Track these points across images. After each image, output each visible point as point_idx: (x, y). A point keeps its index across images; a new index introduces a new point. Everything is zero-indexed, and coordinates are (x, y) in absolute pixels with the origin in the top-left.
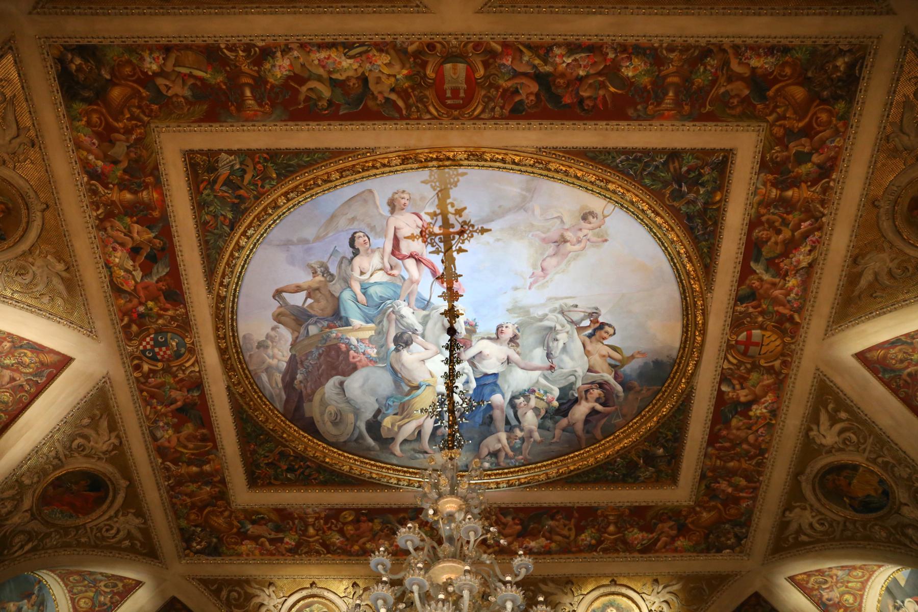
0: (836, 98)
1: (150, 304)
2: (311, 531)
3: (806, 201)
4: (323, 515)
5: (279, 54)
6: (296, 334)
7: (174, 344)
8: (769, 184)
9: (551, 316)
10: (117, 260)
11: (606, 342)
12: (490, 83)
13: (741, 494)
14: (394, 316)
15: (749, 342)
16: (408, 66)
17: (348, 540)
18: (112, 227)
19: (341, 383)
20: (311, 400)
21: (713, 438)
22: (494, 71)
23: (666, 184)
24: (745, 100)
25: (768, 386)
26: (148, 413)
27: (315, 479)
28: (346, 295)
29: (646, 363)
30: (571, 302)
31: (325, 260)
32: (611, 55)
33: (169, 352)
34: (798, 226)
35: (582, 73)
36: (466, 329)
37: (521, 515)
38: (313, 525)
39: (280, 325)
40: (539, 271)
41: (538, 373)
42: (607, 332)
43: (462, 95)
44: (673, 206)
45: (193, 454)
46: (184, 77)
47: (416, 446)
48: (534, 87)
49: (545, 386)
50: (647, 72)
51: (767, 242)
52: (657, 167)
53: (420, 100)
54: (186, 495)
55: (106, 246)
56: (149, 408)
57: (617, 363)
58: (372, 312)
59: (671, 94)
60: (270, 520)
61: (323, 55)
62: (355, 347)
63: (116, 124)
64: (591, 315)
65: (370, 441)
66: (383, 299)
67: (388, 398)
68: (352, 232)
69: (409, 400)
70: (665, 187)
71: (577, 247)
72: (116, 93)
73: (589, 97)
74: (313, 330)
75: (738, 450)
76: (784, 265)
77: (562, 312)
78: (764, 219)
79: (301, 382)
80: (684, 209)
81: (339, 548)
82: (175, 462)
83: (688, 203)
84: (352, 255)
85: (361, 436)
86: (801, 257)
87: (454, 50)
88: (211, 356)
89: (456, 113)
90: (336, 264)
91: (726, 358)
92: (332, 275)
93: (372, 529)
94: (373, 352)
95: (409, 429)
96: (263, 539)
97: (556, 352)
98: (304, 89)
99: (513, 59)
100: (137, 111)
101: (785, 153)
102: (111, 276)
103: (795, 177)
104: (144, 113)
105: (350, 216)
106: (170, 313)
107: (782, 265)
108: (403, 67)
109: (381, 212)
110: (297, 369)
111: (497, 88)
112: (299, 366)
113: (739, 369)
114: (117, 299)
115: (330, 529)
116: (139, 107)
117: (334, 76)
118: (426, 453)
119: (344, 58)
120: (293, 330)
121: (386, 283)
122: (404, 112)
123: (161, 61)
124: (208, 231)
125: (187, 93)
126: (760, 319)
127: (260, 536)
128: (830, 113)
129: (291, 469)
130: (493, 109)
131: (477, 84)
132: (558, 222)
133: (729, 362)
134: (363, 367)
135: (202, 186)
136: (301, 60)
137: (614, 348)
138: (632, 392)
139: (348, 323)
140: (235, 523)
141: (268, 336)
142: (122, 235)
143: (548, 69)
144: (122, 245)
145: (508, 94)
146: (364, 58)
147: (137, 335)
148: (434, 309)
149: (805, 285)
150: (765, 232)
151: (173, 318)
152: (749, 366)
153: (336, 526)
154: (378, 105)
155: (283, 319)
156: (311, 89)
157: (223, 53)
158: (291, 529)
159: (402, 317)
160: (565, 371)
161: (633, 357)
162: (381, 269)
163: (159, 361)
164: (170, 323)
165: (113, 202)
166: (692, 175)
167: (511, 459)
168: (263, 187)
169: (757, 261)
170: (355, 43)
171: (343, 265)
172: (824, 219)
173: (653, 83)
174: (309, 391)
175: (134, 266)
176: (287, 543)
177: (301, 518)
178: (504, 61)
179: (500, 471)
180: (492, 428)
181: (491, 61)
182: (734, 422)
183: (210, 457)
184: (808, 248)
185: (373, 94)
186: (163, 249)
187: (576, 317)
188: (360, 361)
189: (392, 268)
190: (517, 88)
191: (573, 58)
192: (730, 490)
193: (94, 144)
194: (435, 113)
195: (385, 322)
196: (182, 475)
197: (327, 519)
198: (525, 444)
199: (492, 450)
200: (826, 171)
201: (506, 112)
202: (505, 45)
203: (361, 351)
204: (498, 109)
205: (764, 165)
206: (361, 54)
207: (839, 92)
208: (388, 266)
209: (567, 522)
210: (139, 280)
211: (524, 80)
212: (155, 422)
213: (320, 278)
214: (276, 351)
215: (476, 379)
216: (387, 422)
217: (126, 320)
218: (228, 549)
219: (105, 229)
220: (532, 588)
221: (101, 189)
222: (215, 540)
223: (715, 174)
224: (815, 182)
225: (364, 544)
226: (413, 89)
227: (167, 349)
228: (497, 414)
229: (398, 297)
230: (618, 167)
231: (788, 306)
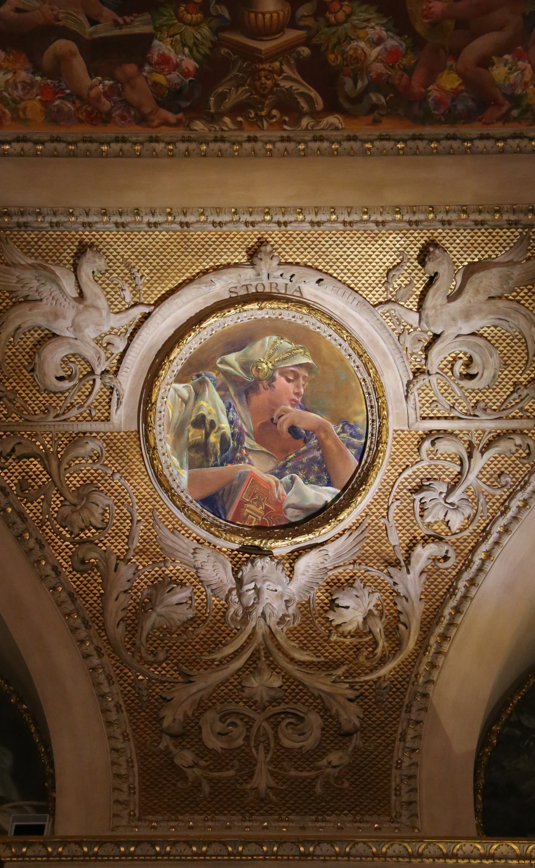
17: (417, 44)
81: (378, 84)
96: (62, 45)
127: (53, 31)
176: (165, 60)
225: (485, 62)
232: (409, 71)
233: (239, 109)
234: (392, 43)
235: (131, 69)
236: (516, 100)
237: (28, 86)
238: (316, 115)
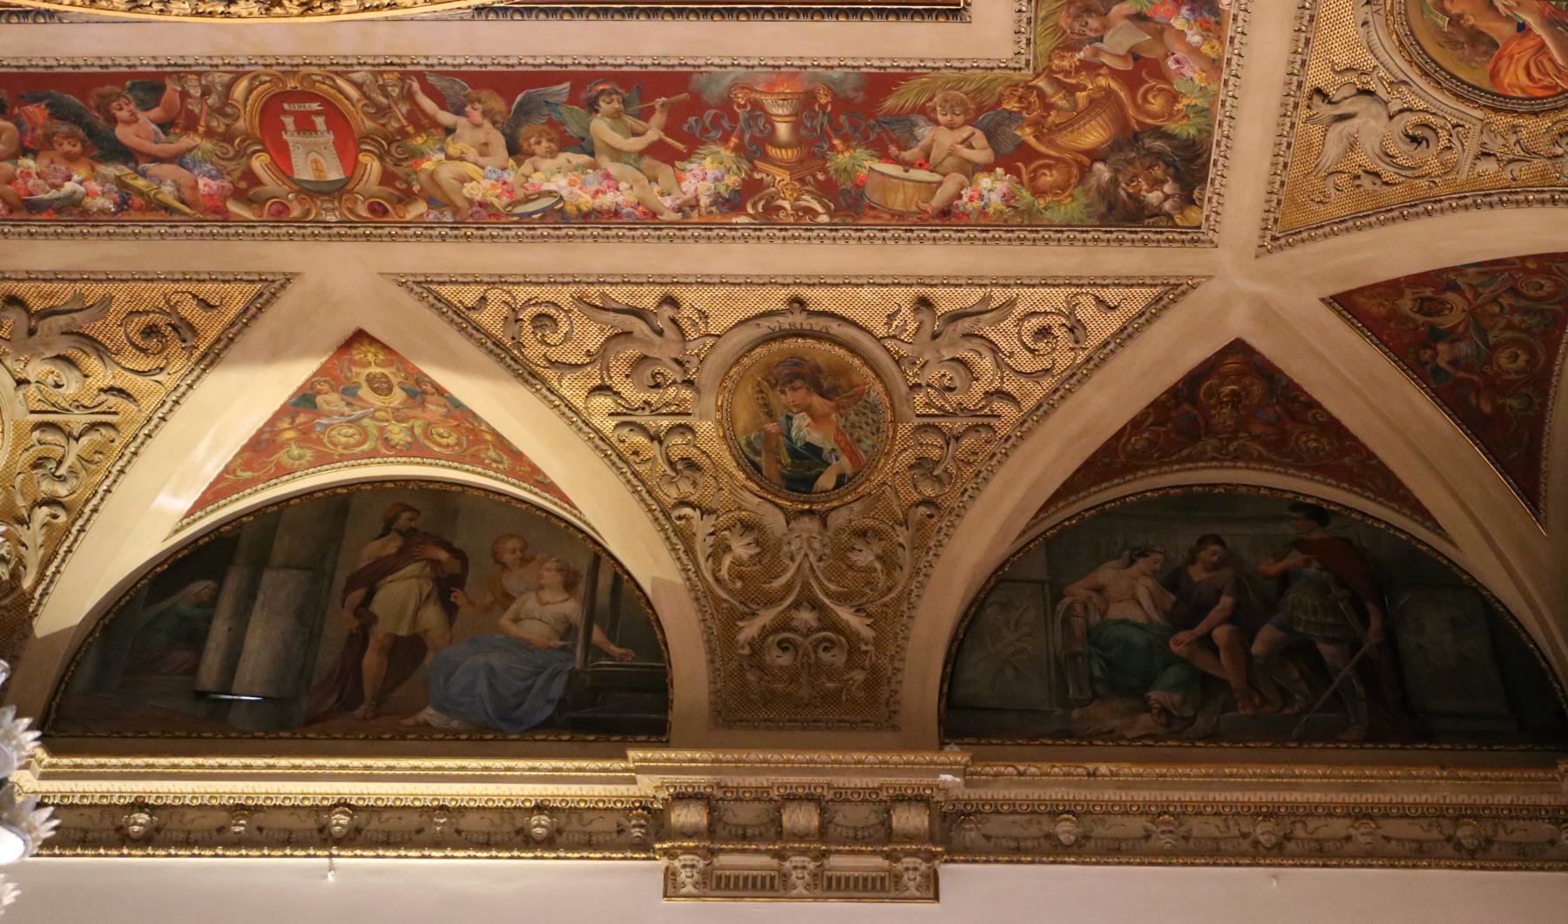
5: (704, 201)
12: (231, 142)
16: (423, 177)
22: (231, 165)
43: (289, 121)
46: (925, 162)
48: (123, 133)
53: (382, 111)
61: (608, 200)
63: (1113, 85)
72: (1094, 135)
89: (291, 84)
98: (653, 134)
99: (195, 187)
100: (1058, 100)
104: (1042, 95)
108: (432, 175)
111: (210, 133)
116: (1048, 107)
119: (564, 193)
122: (416, 86)
123: (966, 193)
125: (925, 132)
130: (206, 92)
131: (261, 142)
136: (656, 189)
145: (181, 122)
146: (520, 194)
154: (479, 101)
156: (635, 134)
157: (825, 206)
170: (541, 221)
178: (214, 184)
181: (243, 185)
185: (494, 123)
190: (166, 133)
193: (1177, 61)
194: (341, 82)
201: (172, 88)
206: (527, 200)
211: (155, 148)
226: (406, 135)
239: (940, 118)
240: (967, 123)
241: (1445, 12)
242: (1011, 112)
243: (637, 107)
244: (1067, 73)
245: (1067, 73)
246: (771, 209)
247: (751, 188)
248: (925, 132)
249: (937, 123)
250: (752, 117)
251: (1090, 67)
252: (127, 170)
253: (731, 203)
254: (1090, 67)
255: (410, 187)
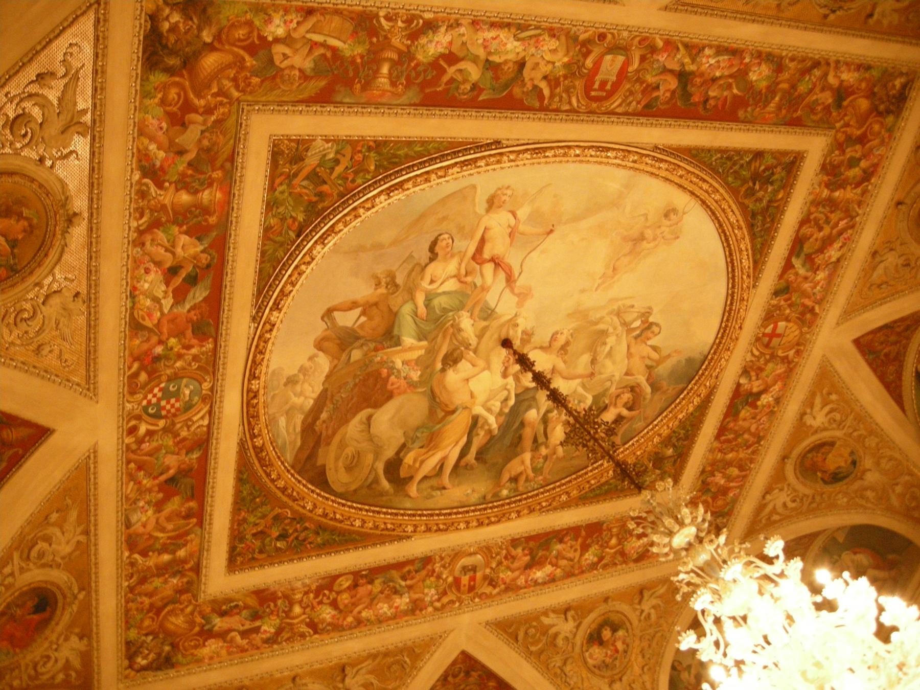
0: (888, 112)
1: (173, 341)
2: (297, 609)
3: (848, 202)
4: (314, 587)
6: (336, 361)
7: (187, 392)
8: (823, 185)
9: (608, 319)
10: (146, 286)
11: (649, 343)
13: (732, 484)
14: (451, 330)
15: (773, 335)
16: (571, 54)
17: (341, 611)
18: (153, 240)
19: (369, 418)
20: (328, 444)
21: (722, 430)
23: (745, 181)
24: (827, 109)
25: (779, 375)
26: (129, 491)
27: (310, 543)
28: (407, 309)
29: (679, 362)
30: (628, 303)
31: (394, 269)
32: (747, 60)
33: (177, 405)
34: (837, 224)
35: (718, 74)
36: (522, 339)
37: (532, 544)
38: (300, 602)
39: (321, 354)
40: (610, 272)
41: (578, 381)
42: (653, 332)
43: (608, 87)
44: (743, 203)
45: (169, 538)
46: (315, 44)
47: (434, 482)
49: (582, 395)
50: (768, 77)
51: (809, 239)
52: (742, 166)
53: (567, 90)
54: (146, 595)
55: (137, 267)
56: (132, 483)
57: (654, 364)
58: (427, 327)
59: (777, 99)
60: (246, 607)
61: (493, 33)
62: (399, 371)
64: (643, 315)
65: (385, 484)
66: (445, 311)
67: (418, 429)
68: (436, 234)
69: (440, 429)
70: (742, 185)
71: (652, 245)
73: (714, 97)
74: (356, 355)
75: (740, 440)
76: (818, 261)
77: (618, 314)
78: (812, 217)
79: (324, 422)
80: (751, 206)
81: (329, 624)
82: (144, 554)
83: (756, 201)
84: (428, 261)
85: (376, 481)
86: (833, 253)
87: (621, 42)
88: (231, 405)
90: (405, 273)
91: (752, 352)
92: (397, 286)
93: (370, 593)
94: (415, 375)
95: (432, 462)
96: (233, 634)
97: (600, 358)
99: (668, 56)
101: (842, 158)
102: (132, 308)
103: (844, 180)
105: (440, 215)
106: (194, 351)
107: (816, 260)
108: (566, 55)
109: (477, 210)
110: (324, 404)
112: (328, 402)
113: (758, 361)
114: (131, 339)
115: (321, 603)
117: (491, 59)
118: (444, 488)
119: (512, 39)
120: (334, 357)
121: (456, 292)
122: (546, 102)
124: (269, 239)
125: (308, 65)
126: (788, 311)
127: (230, 630)
128: (882, 124)
129: (283, 536)
130: (631, 103)
132: (643, 219)
133: (753, 355)
134: (399, 394)
135: (278, 181)
136: (464, 39)
137: (655, 348)
138: (659, 393)
139: (398, 343)
140: (199, 620)
141: (302, 369)
142: (162, 251)
143: (693, 68)
144: (158, 264)
145: (649, 89)
146: (532, 41)
147: (143, 387)
148: (496, 318)
149: (830, 279)
150: (810, 230)
151: (195, 358)
152: (768, 357)
153: (329, 598)
154: (523, 92)
155: (326, 344)
156: (460, 71)
157: (379, 21)
158: (272, 613)
159: (460, 330)
160: (603, 376)
161: (669, 356)
162: (455, 276)
163: (161, 417)
164: (190, 364)
165: (164, 207)
166: (767, 173)
167: (531, 481)
168: (353, 181)
169: (798, 256)
171: (414, 273)
172: (857, 219)
173: (768, 88)
174: (330, 432)
175: (166, 292)
176: (265, 631)
177: (285, 596)
179: (518, 498)
180: (519, 449)
181: (649, 56)
182: (743, 414)
183: (189, 538)
184: (840, 244)
185: (523, 81)
186: (208, 266)
187: (628, 318)
188: (398, 388)
189: (467, 275)
191: (717, 59)
192: (722, 482)
195: (439, 339)
196: (149, 568)
197: (318, 592)
198: (547, 463)
199: (513, 474)
200: (867, 176)
202: (668, 43)
203: (403, 374)
204: (634, 103)
205: (823, 167)
206: (531, 37)
207: (891, 107)
208: (463, 272)
209: (573, 543)
210: (166, 311)
212: (135, 502)
213: (382, 290)
214: (306, 386)
215: (517, 395)
216: (409, 459)
217: (136, 366)
218: (184, 656)
219: (143, 244)
220: (534, 624)
221: (153, 189)
222: (167, 648)
223: (784, 174)
224: (858, 185)
225: (360, 612)
227: (177, 401)
228: (528, 433)
229: (461, 306)
230: (711, 164)
231: (813, 298)
232: (338, 619)
233: (288, 639)
234: (333, 612)
235: (254, 635)
236: (368, 620)
237: (222, 647)
238: (311, 636)
239: (297, 73)
240: (282, 70)
241: (26, 219)
242: (257, 76)
243: (453, 86)
244: (221, 104)
245: (221, 104)
246: (409, 21)
247: (414, 36)
248: (308, 65)
249: (300, 70)
250: (398, 77)
251: (209, 111)
252: (687, 68)
253: (431, 26)
254: (209, 111)
255: (580, 50)
